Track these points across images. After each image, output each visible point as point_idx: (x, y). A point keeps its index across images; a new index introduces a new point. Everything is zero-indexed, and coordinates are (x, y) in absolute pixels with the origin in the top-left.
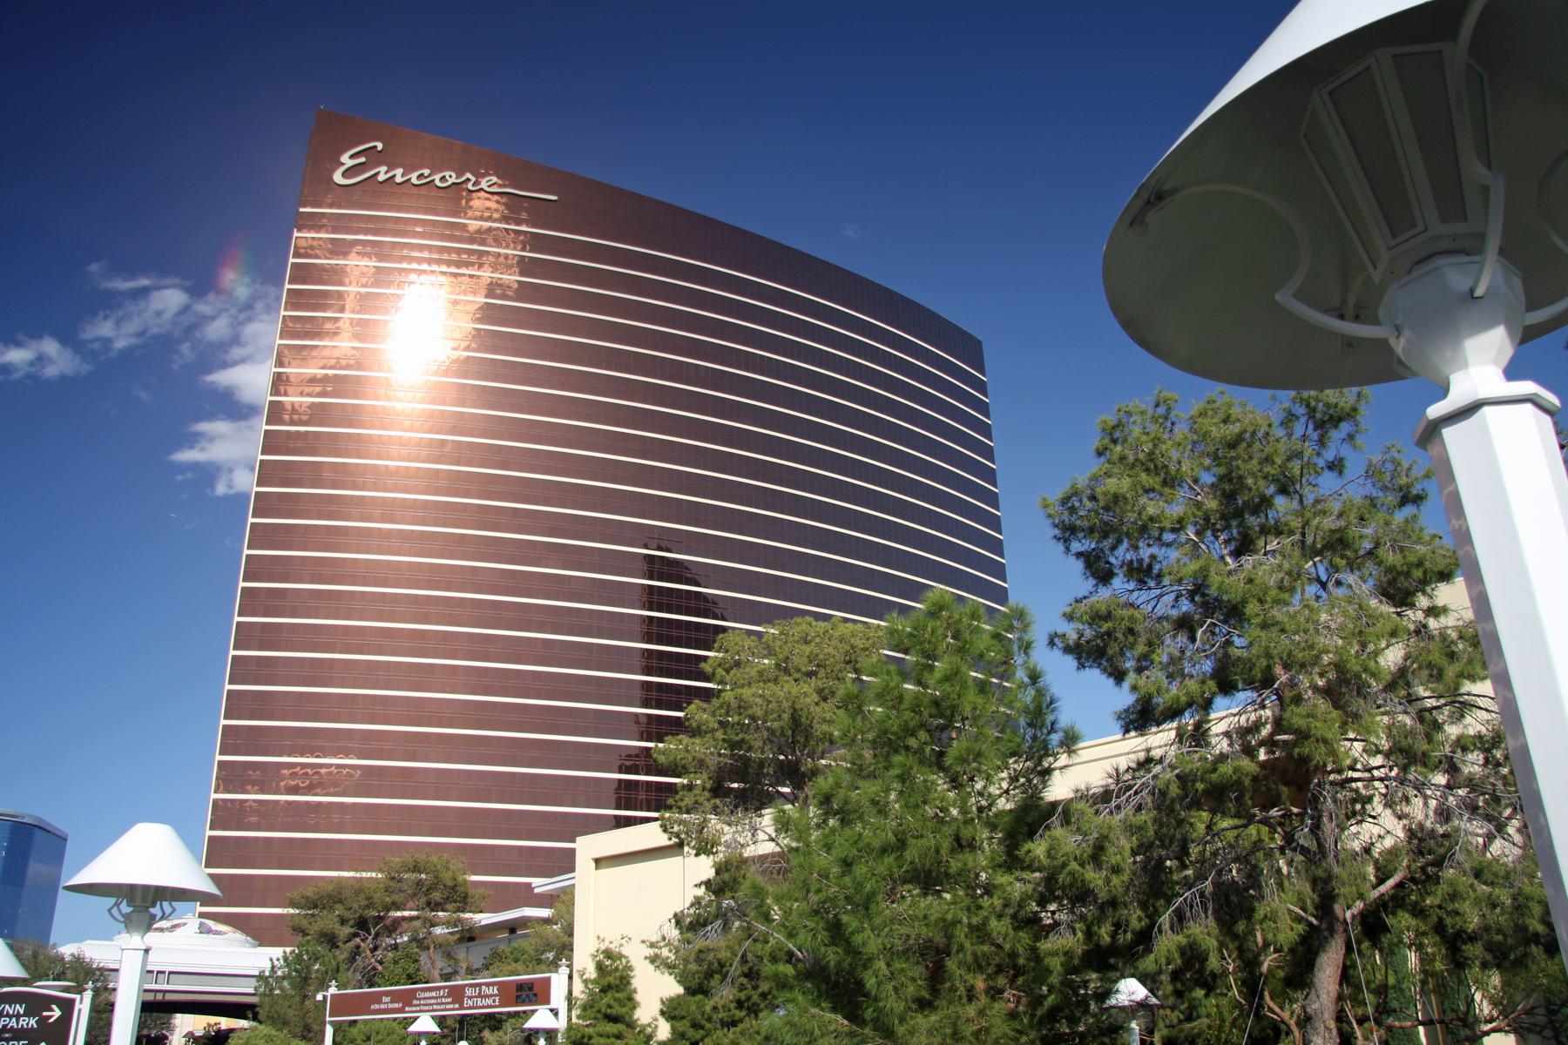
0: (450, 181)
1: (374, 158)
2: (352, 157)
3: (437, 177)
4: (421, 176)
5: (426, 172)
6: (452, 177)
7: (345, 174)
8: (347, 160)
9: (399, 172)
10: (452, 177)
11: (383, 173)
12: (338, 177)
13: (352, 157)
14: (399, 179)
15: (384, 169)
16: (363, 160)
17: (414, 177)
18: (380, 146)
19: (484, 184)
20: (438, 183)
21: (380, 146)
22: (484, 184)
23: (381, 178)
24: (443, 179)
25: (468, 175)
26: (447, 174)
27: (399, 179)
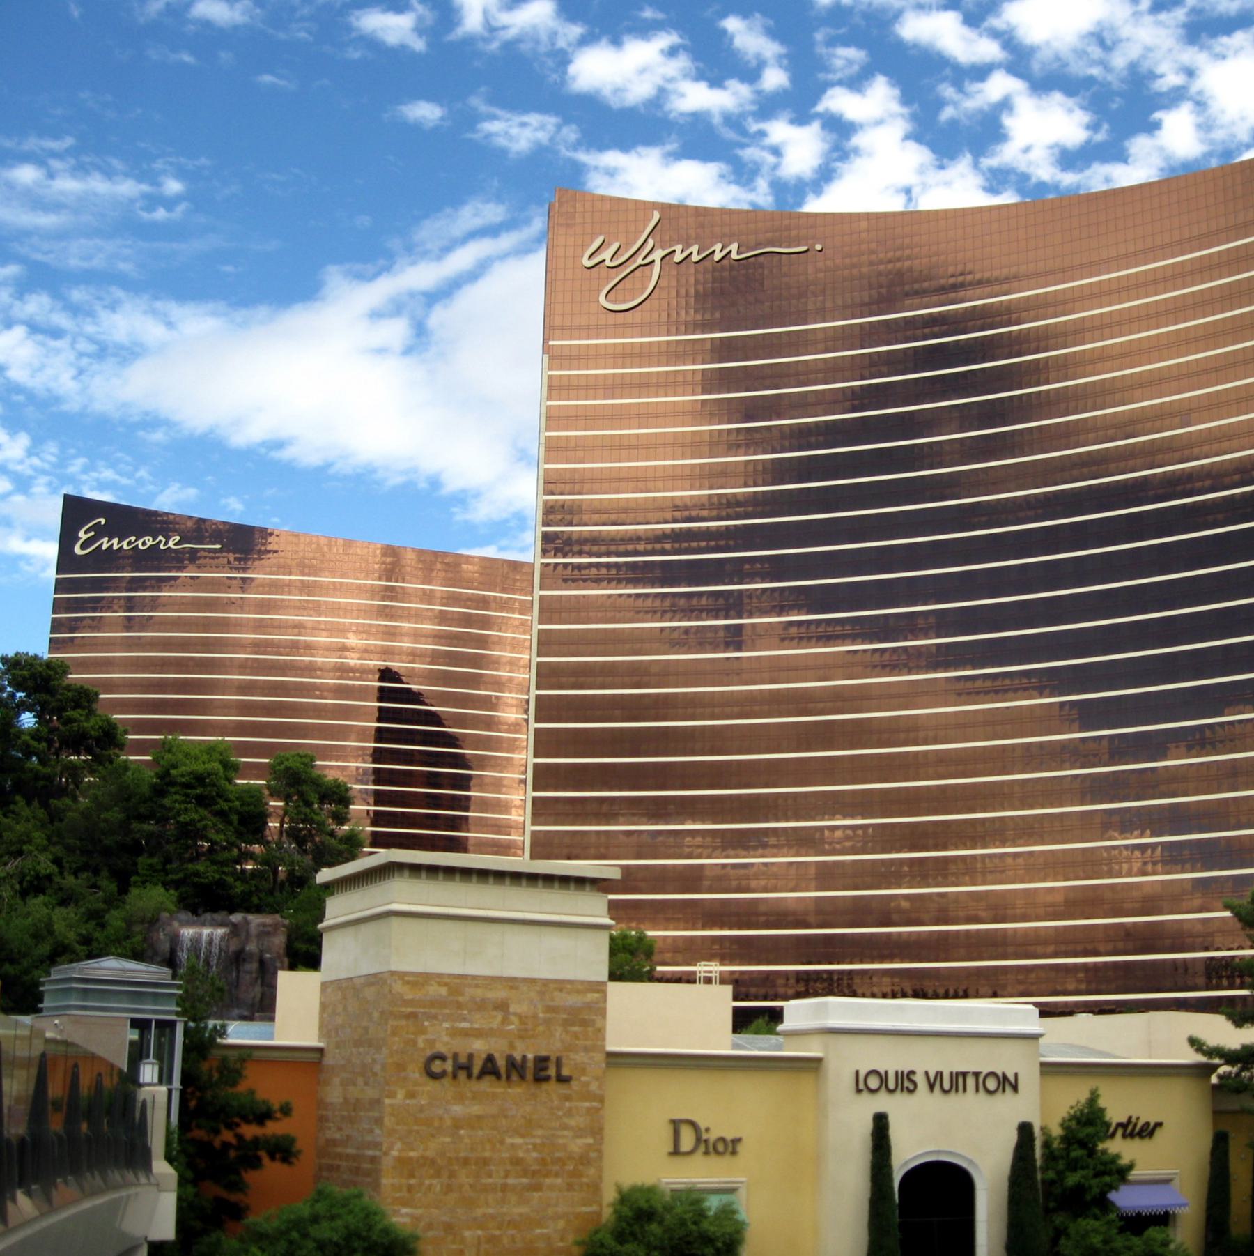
0: (149, 544)
1: (99, 532)
2: (86, 532)
3: (140, 542)
4: (129, 543)
5: (133, 539)
6: (149, 541)
7: (83, 547)
8: (83, 535)
9: (115, 541)
10: (149, 541)
11: (105, 543)
12: (78, 550)
13: (86, 532)
14: (115, 547)
15: (106, 539)
16: (92, 533)
17: (125, 544)
18: (103, 521)
19: (171, 544)
20: (141, 547)
21: (103, 521)
22: (171, 544)
23: (104, 547)
24: (144, 544)
25: (160, 538)
26: (146, 538)
27: (115, 547)
